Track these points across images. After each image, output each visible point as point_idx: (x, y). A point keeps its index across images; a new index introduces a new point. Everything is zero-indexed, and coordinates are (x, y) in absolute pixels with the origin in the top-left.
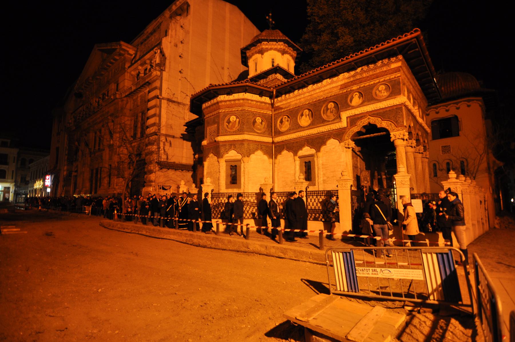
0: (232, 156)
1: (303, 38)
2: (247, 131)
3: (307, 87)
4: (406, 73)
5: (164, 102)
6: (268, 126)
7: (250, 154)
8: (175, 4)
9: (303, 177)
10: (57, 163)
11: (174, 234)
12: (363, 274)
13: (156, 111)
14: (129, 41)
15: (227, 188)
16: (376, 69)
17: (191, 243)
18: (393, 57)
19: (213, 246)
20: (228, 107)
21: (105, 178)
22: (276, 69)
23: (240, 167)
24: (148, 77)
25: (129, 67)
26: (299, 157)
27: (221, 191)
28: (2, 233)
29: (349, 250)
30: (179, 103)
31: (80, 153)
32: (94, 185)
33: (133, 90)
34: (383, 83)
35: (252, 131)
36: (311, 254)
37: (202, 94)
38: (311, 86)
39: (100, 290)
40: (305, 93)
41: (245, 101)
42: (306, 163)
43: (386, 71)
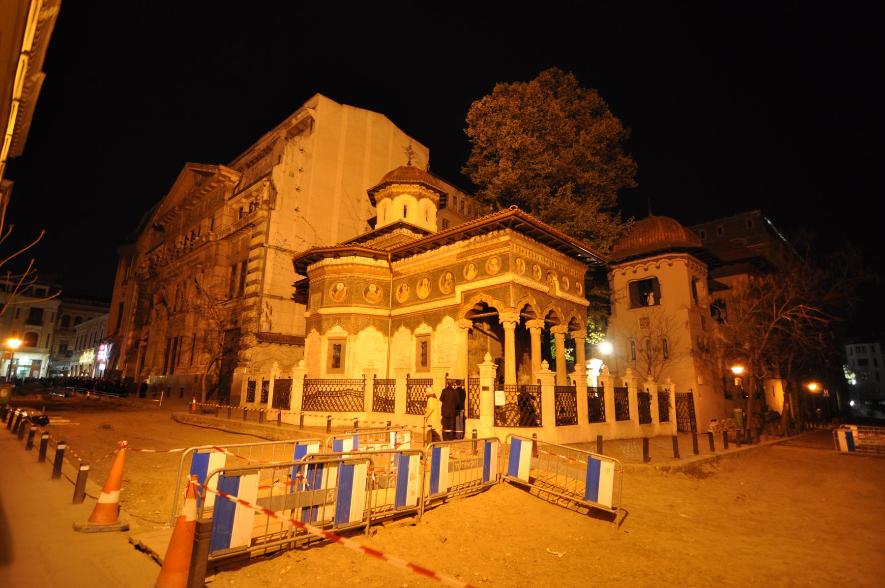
6: (384, 295)
7: (358, 331)
8: (295, 117)
10: (118, 326)
11: (256, 428)
13: (259, 263)
15: (328, 372)
20: (335, 272)
25: (230, 199)
26: (417, 336)
27: (321, 377)
31: (154, 314)
32: (170, 362)
33: (231, 232)
35: (362, 302)
40: (423, 259)
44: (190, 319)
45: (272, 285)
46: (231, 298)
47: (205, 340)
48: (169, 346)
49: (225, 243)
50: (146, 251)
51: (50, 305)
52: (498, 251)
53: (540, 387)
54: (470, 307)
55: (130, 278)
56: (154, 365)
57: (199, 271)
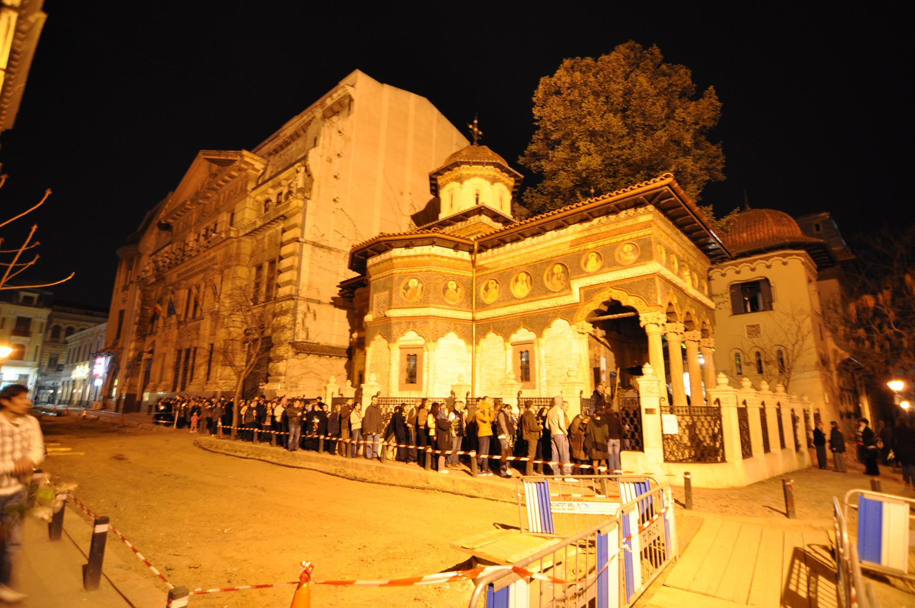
6: (466, 295)
7: (438, 338)
10: (118, 336)
11: (317, 460)
15: (401, 389)
16: (618, 222)
17: (343, 475)
20: (407, 266)
21: (201, 365)
23: (422, 357)
24: (283, 208)
27: (392, 395)
31: (161, 322)
33: (257, 226)
35: (441, 302)
38: (529, 239)
39: (226, 531)
40: (519, 249)
41: (432, 258)
43: (632, 226)
44: (206, 325)
45: (310, 287)
46: (255, 301)
47: (225, 352)
48: (179, 358)
49: (248, 240)
50: (150, 252)
51: (40, 315)
55: (131, 282)
56: (161, 381)
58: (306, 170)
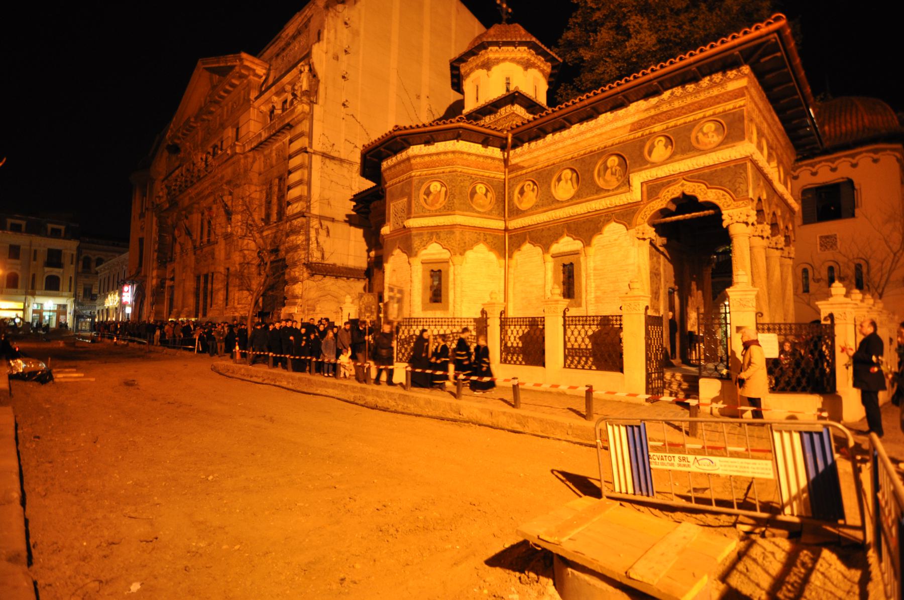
0: (433, 254)
1: (563, 37)
2: (459, 210)
3: (569, 128)
4: (757, 99)
5: (316, 160)
7: (465, 251)
9: (558, 290)
11: (334, 386)
12: (663, 464)
13: (303, 174)
14: (255, 52)
15: (424, 309)
16: (698, 92)
17: (363, 403)
18: (731, 69)
19: (399, 409)
20: (427, 166)
21: (219, 290)
22: (514, 97)
23: (447, 272)
25: (256, 98)
27: (414, 315)
28: (56, 380)
29: (637, 423)
30: (342, 161)
31: (178, 248)
32: (201, 302)
33: (263, 139)
34: (711, 118)
35: (469, 209)
36: (570, 427)
37: (381, 145)
38: (576, 126)
39: (210, 478)
40: (565, 139)
42: (564, 265)
43: (717, 97)
44: (220, 251)
47: (241, 276)
50: (162, 177)
51: (69, 247)
52: (720, 109)
53: (832, 326)
54: (659, 204)
55: (147, 209)
56: (183, 307)
57: (226, 193)
58: (310, 70)
